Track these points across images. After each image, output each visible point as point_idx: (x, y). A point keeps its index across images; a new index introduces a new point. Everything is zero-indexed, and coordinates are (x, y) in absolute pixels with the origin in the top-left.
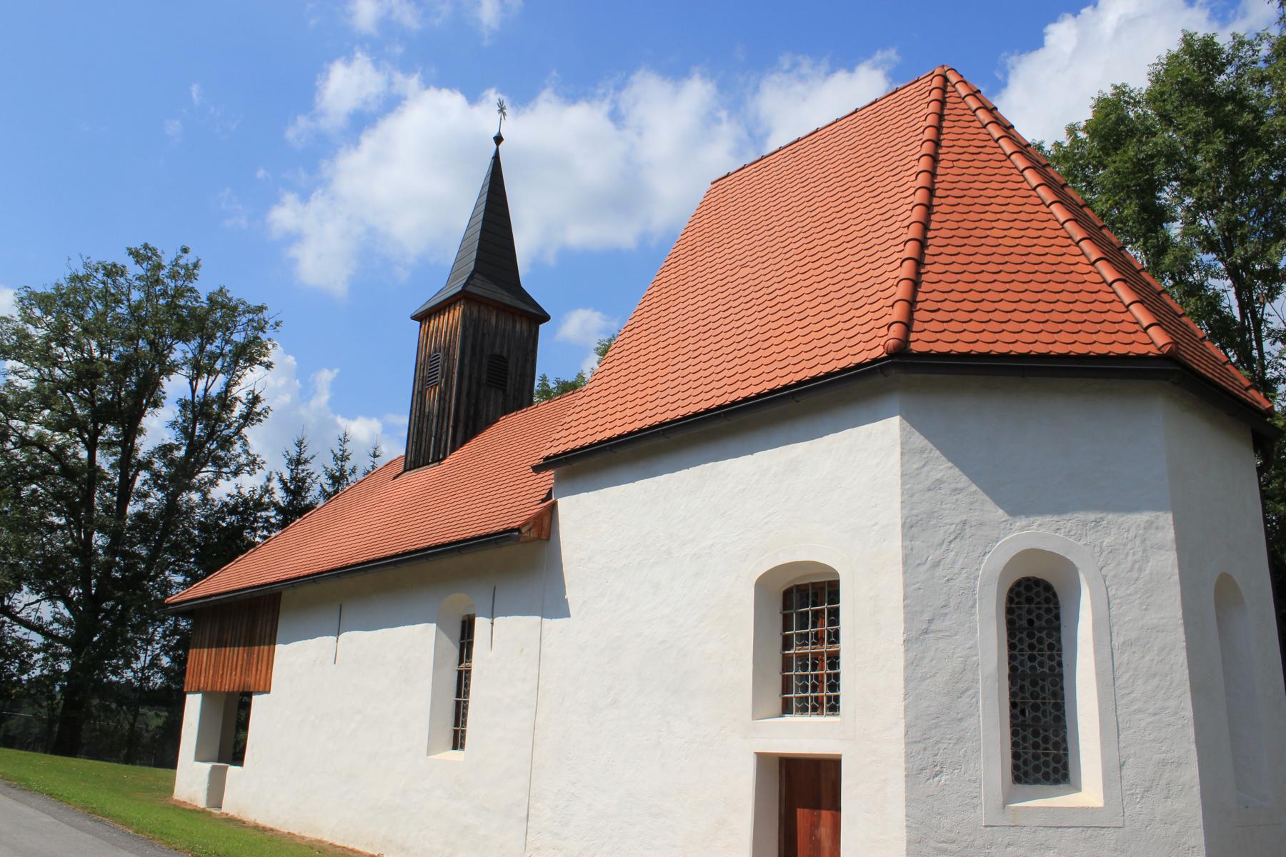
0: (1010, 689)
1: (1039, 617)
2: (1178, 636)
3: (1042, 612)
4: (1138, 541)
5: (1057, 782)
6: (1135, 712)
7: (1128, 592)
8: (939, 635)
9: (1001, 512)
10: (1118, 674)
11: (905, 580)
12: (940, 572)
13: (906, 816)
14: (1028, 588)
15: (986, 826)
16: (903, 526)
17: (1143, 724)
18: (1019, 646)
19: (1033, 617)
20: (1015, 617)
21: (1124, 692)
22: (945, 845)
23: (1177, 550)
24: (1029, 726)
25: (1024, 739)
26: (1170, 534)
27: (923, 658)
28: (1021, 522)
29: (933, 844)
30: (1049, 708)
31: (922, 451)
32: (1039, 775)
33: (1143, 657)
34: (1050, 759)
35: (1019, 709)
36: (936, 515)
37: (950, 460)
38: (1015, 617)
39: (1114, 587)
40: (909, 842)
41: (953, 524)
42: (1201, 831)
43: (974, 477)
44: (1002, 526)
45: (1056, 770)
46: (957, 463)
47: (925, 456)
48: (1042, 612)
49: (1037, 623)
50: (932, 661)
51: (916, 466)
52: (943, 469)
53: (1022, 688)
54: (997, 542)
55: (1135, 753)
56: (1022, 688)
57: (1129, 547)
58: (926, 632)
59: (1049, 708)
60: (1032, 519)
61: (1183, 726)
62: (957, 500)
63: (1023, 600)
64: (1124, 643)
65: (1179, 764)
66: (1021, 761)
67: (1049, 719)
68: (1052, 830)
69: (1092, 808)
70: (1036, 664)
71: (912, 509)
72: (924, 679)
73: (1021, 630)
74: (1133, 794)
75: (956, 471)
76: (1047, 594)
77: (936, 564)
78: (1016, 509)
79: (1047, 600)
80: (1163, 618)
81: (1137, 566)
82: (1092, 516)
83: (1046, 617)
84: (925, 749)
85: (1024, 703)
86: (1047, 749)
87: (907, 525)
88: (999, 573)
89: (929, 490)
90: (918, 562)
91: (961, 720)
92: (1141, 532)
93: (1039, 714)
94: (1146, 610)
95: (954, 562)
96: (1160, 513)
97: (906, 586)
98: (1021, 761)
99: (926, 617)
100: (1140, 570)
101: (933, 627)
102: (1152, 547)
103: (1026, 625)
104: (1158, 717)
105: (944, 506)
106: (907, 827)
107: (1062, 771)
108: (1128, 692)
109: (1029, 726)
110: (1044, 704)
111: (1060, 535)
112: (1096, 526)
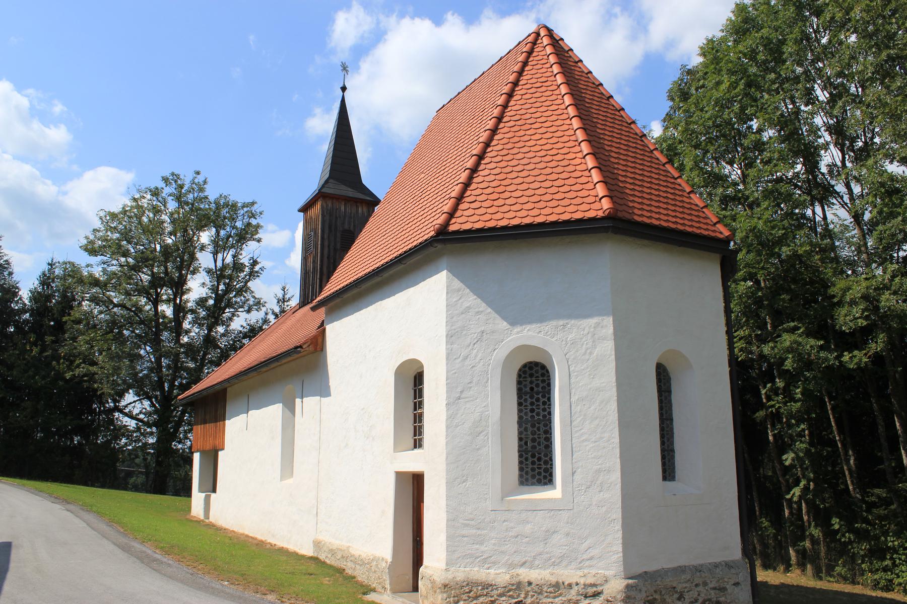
0: (518, 430)
1: (537, 386)
2: (613, 393)
3: (539, 382)
4: (590, 335)
5: (545, 484)
6: (583, 441)
7: (583, 368)
8: (467, 400)
9: (505, 323)
10: (573, 418)
11: (447, 369)
12: (467, 362)
13: (447, 505)
14: (531, 368)
15: (492, 511)
16: (447, 336)
17: (588, 448)
18: (524, 404)
19: (533, 386)
20: (522, 386)
21: (576, 429)
22: (468, 522)
23: (614, 339)
24: (529, 451)
25: (526, 459)
26: (611, 330)
27: (457, 414)
28: (518, 329)
29: (461, 521)
30: (542, 440)
31: (459, 290)
32: (535, 480)
33: (590, 407)
34: (542, 471)
35: (524, 441)
36: (466, 328)
37: (475, 294)
38: (522, 386)
39: (574, 365)
40: (448, 520)
41: (475, 333)
42: (620, 510)
43: (490, 304)
44: (506, 332)
45: (545, 477)
46: (480, 296)
47: (460, 293)
48: (539, 382)
49: (536, 389)
50: (462, 415)
51: (455, 300)
52: (471, 300)
53: (526, 429)
54: (502, 342)
55: (582, 466)
56: (526, 429)
57: (584, 340)
58: (459, 398)
59: (542, 440)
60: (524, 327)
61: (613, 448)
62: (479, 318)
63: (527, 376)
64: (578, 399)
65: (609, 471)
66: (524, 472)
67: (542, 447)
68: (530, 512)
69: (555, 499)
70: (534, 414)
71: (452, 326)
72: (457, 426)
73: (526, 393)
74: (579, 490)
75: (479, 300)
76: (543, 371)
77: (466, 358)
78: (514, 322)
79: (543, 375)
80: (603, 383)
81: (588, 351)
82: (561, 322)
83: (541, 385)
84: (457, 467)
85: (527, 438)
86: (540, 465)
87: (450, 336)
88: (503, 361)
89: (462, 313)
90: (455, 357)
91: (478, 449)
92: (592, 330)
93: (536, 444)
94: (593, 378)
95: (476, 356)
96: (604, 317)
97: (448, 372)
98: (524, 472)
99: (459, 389)
100: (591, 353)
101: (463, 396)
102: (599, 339)
103: (529, 391)
104: (597, 443)
105: (471, 323)
106: (447, 511)
107: (549, 478)
108: (580, 428)
109: (529, 451)
110: (539, 438)
111: (541, 335)
112: (563, 328)
